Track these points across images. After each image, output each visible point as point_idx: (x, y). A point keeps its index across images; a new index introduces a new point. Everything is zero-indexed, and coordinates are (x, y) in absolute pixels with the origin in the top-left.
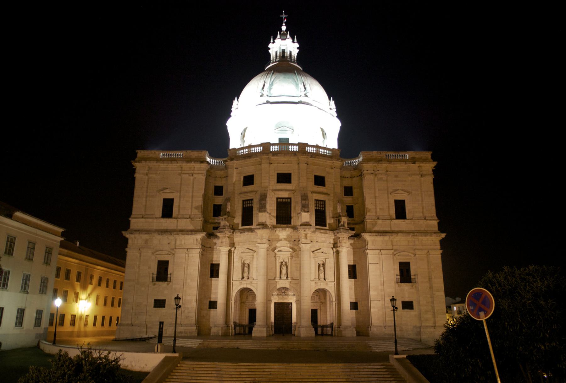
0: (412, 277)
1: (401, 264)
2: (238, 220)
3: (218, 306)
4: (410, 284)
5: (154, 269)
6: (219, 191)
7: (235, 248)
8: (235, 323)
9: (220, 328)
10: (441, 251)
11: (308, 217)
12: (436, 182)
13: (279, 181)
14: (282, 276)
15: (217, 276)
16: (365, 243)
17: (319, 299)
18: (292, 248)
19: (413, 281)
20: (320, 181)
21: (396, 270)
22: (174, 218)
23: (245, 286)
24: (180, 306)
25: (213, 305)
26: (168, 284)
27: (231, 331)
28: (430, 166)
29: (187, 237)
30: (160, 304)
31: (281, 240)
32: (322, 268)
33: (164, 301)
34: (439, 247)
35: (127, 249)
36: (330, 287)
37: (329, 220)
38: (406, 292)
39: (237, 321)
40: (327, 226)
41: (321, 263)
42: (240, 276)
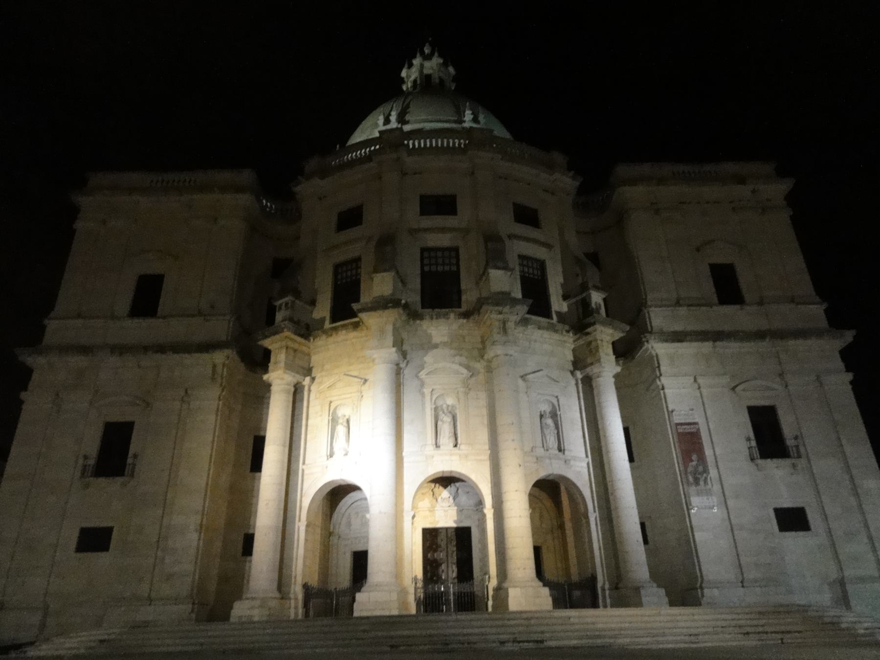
0: (790, 442)
1: (754, 412)
2: (323, 310)
4: (787, 462)
5: (92, 446)
7: (313, 379)
8: (305, 586)
10: (850, 376)
11: (502, 280)
12: (799, 224)
13: (424, 212)
16: (653, 365)
18: (468, 368)
21: (744, 427)
22: (159, 318)
26: (124, 485)
28: (778, 190)
29: (188, 359)
30: (94, 540)
31: (436, 346)
32: (550, 422)
34: (840, 364)
35: (23, 395)
36: (578, 469)
37: (559, 305)
38: (782, 483)
39: (314, 581)
40: (554, 316)
41: (546, 408)
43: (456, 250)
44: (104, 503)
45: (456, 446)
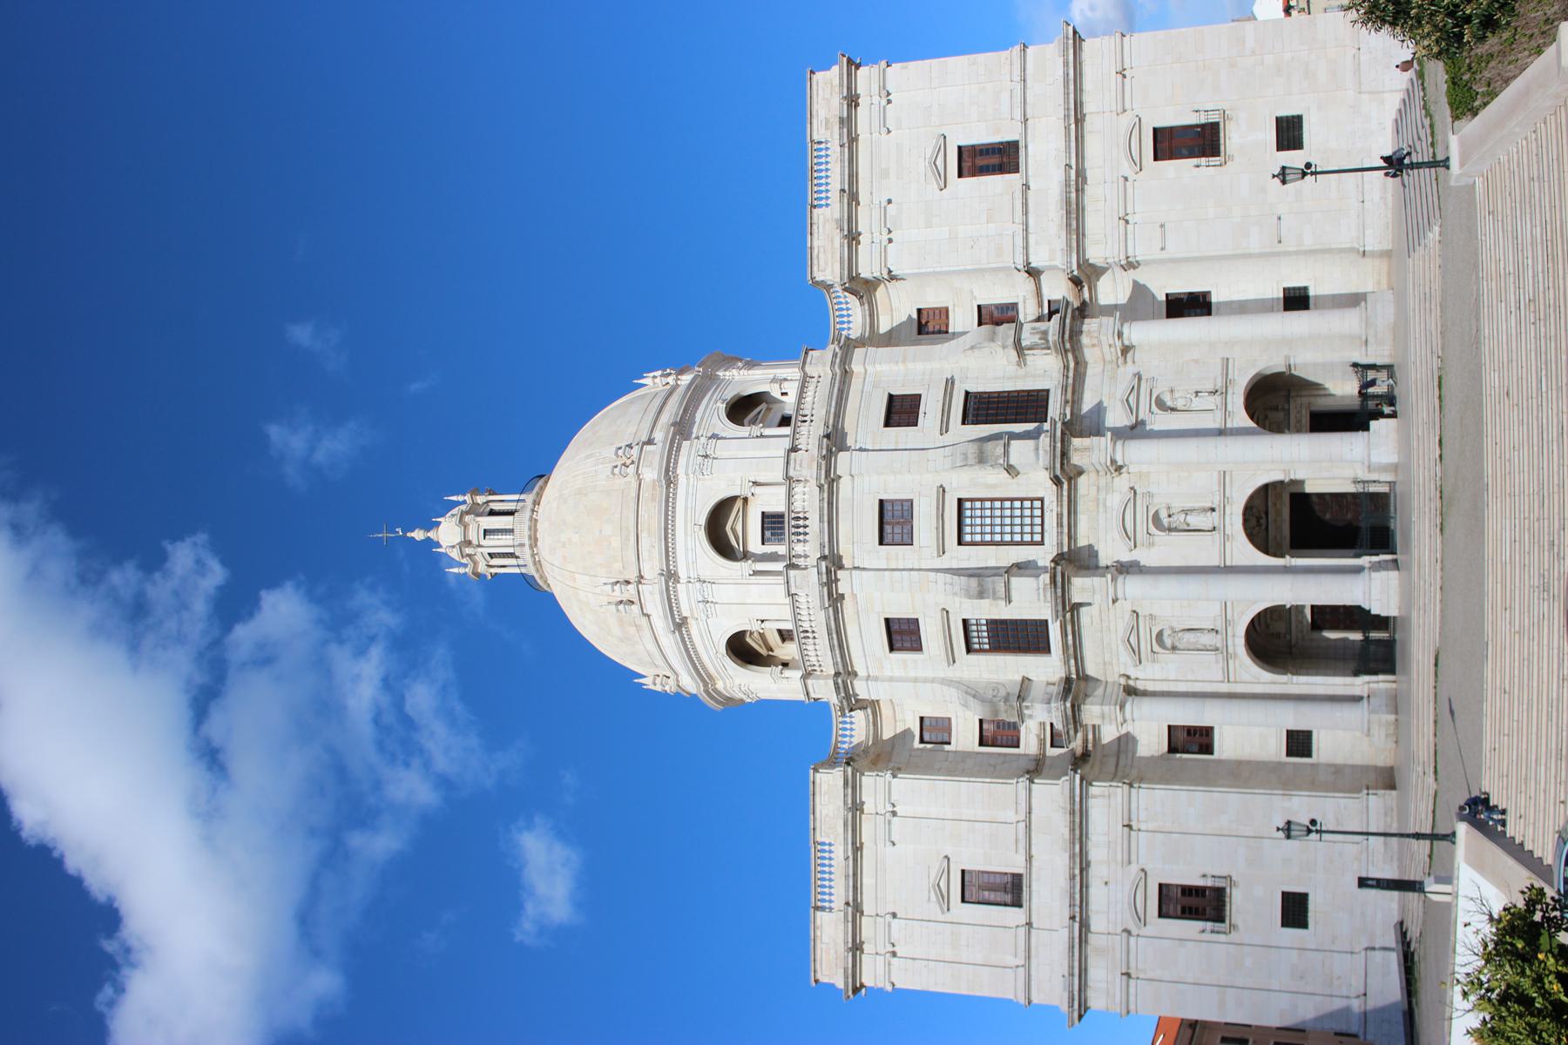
0: (1202, 119)
3: (1300, 725)
6: (935, 731)
8: (1356, 674)
9: (1374, 717)
14: (1210, 527)
15: (1207, 732)
17: (1276, 409)
19: (1213, 118)
20: (902, 411)
23: (1241, 641)
24: (1313, 822)
25: (1299, 743)
27: (1382, 686)
30: (1295, 910)
33: (1286, 896)
42: (1211, 656)
43: (960, 501)
44: (1253, 906)
45: (1213, 510)
